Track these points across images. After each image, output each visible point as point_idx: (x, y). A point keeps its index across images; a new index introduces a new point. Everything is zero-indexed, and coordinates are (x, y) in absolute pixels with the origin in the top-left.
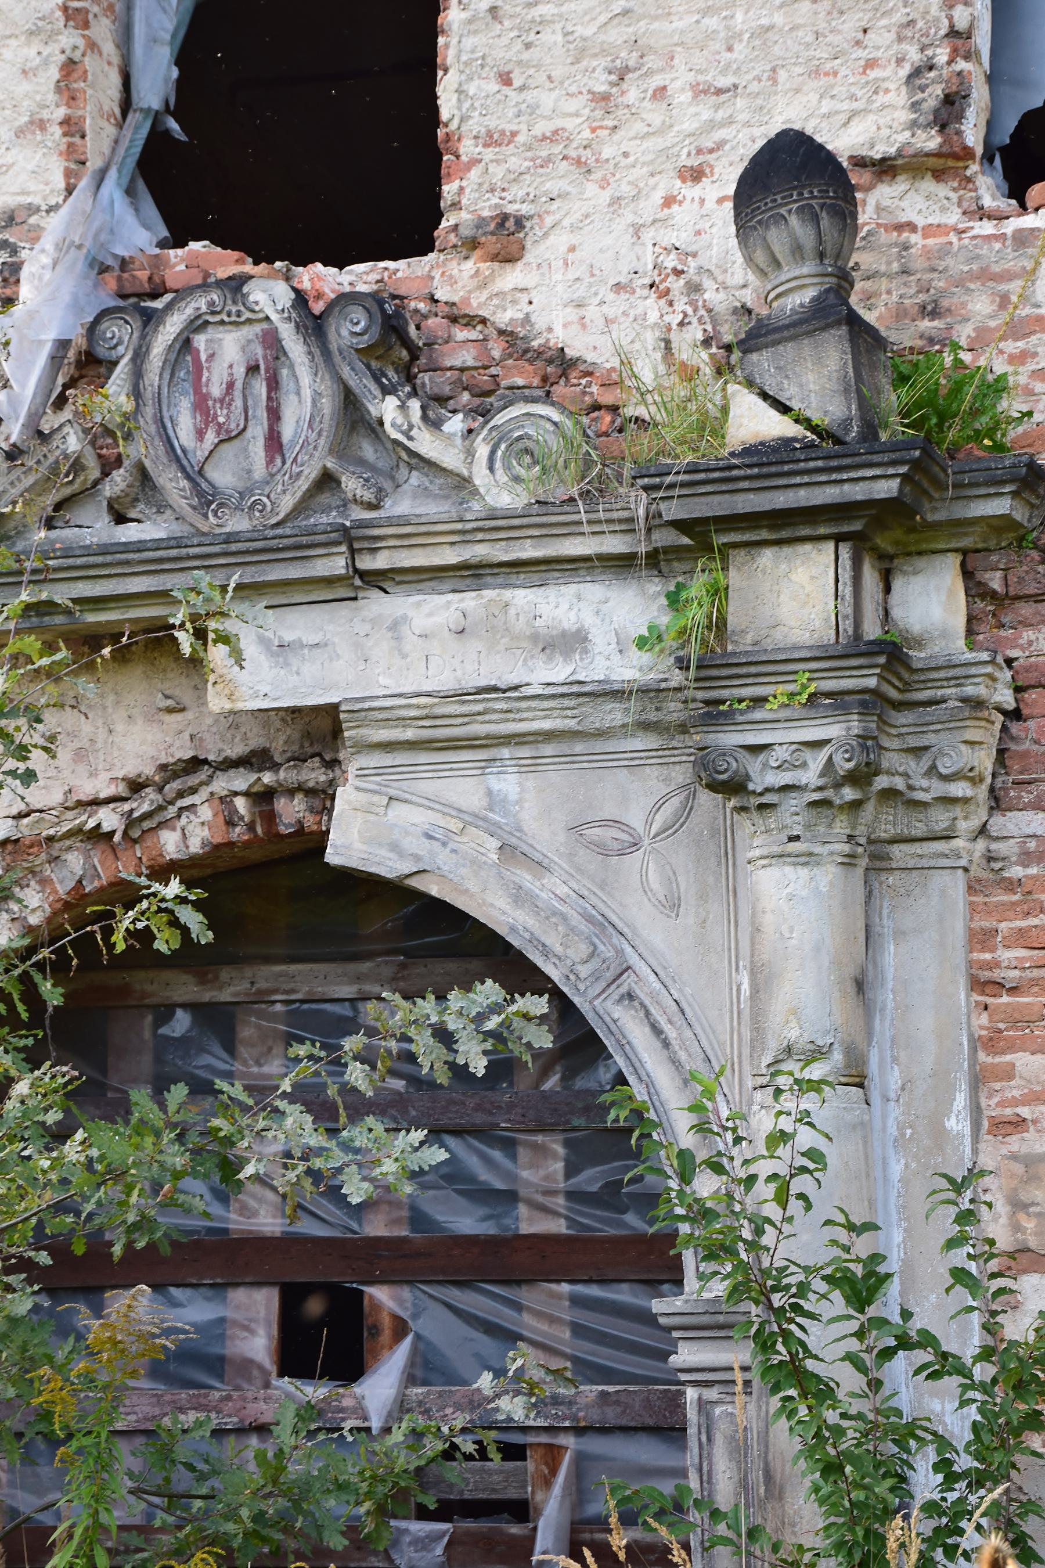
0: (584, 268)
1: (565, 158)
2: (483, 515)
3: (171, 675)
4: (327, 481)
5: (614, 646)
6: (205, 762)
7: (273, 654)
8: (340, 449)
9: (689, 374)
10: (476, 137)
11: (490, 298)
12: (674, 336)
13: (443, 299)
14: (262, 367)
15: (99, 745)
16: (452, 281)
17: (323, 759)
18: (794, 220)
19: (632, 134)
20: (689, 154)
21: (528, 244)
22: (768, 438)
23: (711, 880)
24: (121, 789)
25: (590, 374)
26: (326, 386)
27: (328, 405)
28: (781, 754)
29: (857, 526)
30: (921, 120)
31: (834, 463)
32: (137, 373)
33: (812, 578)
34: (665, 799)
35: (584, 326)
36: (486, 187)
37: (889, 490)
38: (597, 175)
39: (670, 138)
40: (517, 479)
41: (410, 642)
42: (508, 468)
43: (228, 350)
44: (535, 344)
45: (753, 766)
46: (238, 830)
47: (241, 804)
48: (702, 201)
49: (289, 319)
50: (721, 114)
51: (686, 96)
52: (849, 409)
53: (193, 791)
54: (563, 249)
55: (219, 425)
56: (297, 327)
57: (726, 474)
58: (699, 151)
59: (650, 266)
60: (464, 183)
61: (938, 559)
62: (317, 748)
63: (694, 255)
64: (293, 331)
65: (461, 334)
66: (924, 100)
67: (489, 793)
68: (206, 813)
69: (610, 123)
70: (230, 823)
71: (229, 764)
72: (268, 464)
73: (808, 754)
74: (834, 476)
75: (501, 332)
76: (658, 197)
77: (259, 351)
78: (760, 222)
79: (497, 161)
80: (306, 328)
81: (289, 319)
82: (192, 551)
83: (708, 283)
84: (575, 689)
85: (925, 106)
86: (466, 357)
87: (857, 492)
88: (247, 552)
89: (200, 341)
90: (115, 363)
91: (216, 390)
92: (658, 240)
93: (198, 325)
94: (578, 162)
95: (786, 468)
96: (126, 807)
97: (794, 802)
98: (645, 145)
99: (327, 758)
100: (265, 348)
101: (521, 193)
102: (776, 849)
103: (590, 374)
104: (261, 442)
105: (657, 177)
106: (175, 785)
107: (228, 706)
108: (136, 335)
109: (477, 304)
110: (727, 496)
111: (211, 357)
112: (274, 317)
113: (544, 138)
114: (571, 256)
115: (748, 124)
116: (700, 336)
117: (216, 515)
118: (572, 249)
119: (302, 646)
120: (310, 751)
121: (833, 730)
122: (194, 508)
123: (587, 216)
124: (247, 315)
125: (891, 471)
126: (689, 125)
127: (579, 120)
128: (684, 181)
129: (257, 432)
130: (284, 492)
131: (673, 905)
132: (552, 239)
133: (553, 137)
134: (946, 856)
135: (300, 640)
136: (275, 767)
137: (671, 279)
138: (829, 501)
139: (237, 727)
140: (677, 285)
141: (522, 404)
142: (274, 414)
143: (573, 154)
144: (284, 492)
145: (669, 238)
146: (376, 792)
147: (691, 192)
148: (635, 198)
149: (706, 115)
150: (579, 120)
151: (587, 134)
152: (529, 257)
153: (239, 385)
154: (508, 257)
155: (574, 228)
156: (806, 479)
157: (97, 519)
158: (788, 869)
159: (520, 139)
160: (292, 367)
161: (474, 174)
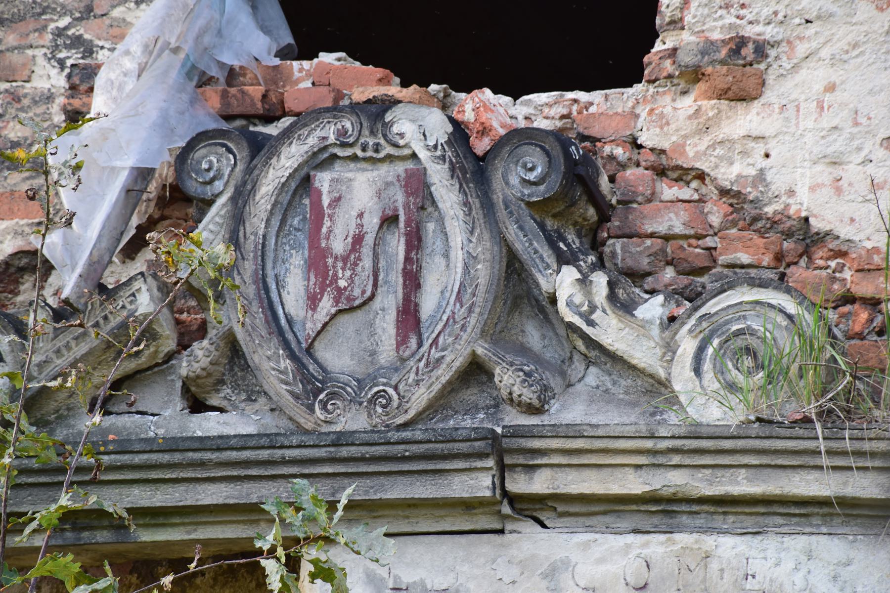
2: (682, 431)
11: (713, 146)
13: (649, 144)
14: (402, 218)
16: (663, 122)
21: (770, 78)
26: (485, 247)
27: (483, 272)
40: (732, 387)
42: (720, 371)
43: (359, 194)
44: (769, 210)
49: (443, 158)
54: (819, 87)
55: (340, 290)
56: (452, 169)
75: (724, 192)
77: (400, 198)
81: (443, 158)
86: (674, 222)
88: (362, 459)
89: (323, 180)
91: (339, 246)
100: (408, 194)
108: (240, 167)
109: (694, 153)
111: (336, 201)
112: (423, 154)
117: (324, 407)
118: (831, 88)
122: (296, 397)
124: (388, 150)
130: (417, 383)
132: (803, 74)
141: (745, 288)
152: (770, 95)
153: (369, 239)
154: (741, 95)
160: (441, 221)
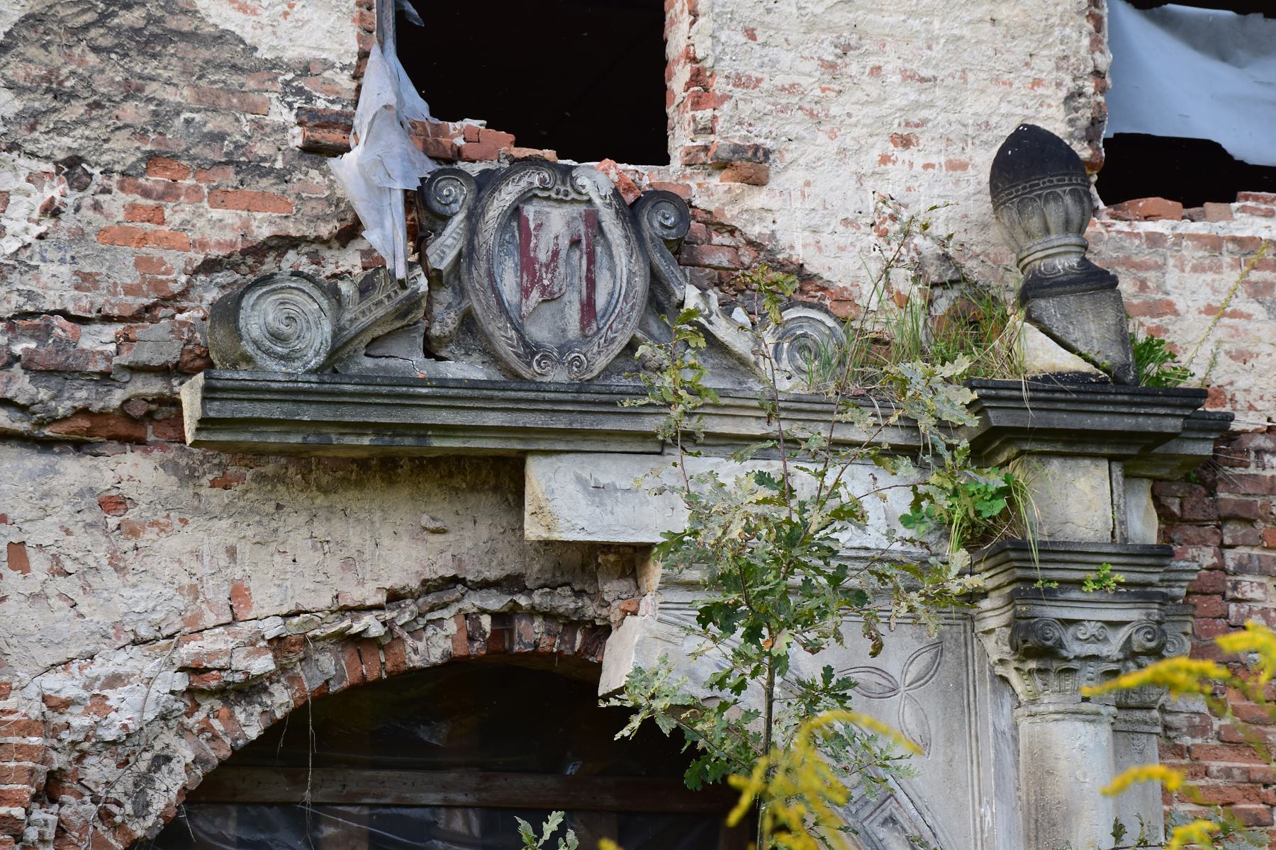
0: (818, 201)
1: (800, 108)
2: (791, 397)
3: (435, 499)
4: (632, 346)
5: (883, 521)
6: (463, 581)
9: (904, 301)
10: (727, 77)
11: (741, 213)
13: (702, 207)
14: (584, 242)
15: (366, 556)
16: (709, 193)
17: (573, 590)
18: (1068, 200)
19: (854, 99)
20: (899, 125)
21: (772, 173)
22: (1064, 371)
23: (956, 726)
24: (381, 598)
25: (823, 289)
26: (639, 268)
27: (640, 284)
28: (1092, 629)
29: (1133, 451)
30: (1076, 133)
31: (1138, 399)
32: (472, 228)
33: (1092, 487)
34: (917, 654)
35: (820, 249)
36: (735, 120)
37: (1175, 427)
38: (827, 127)
39: (884, 109)
40: (800, 370)
42: (791, 359)
43: (554, 224)
44: (780, 257)
45: (1068, 635)
46: (476, 644)
47: (486, 621)
48: (911, 164)
49: (610, 204)
50: (923, 98)
51: (897, 78)
52: (1127, 356)
53: (445, 606)
54: (800, 182)
55: (543, 286)
56: (617, 213)
57: (1050, 395)
58: (907, 124)
59: (872, 210)
60: (717, 113)
61: (1137, 482)
62: (567, 578)
63: (906, 207)
64: (614, 216)
65: (717, 239)
66: (1078, 119)
68: (451, 627)
69: (837, 88)
70: (471, 639)
71: (485, 585)
72: (583, 329)
73: (1109, 632)
74: (1133, 410)
75: (750, 243)
76: (875, 154)
77: (582, 229)
78: (1039, 196)
79: (744, 100)
80: (623, 213)
81: (610, 204)
82: (547, 395)
84: (862, 554)
85: (1078, 123)
86: (722, 259)
87: (1150, 425)
88: (594, 403)
89: (530, 211)
90: (445, 219)
91: (543, 257)
92: (877, 189)
94: (811, 114)
95: (1099, 397)
96: (388, 615)
97: (1093, 669)
98: (865, 111)
99: (576, 588)
100: (587, 227)
101: (765, 130)
102: (1071, 707)
103: (823, 289)
105: (875, 138)
106: (431, 599)
107: (545, 535)
108: (470, 196)
109: (730, 215)
110: (1044, 413)
111: (539, 226)
112: (598, 201)
113: (783, 89)
115: (945, 110)
117: (539, 364)
118: (808, 184)
120: (560, 580)
121: (1135, 615)
122: (519, 356)
123: (819, 159)
124: (573, 195)
125: (1179, 412)
126: (899, 102)
127: (812, 80)
128: (896, 146)
130: (599, 353)
132: (790, 173)
133: (791, 89)
134: (1146, 723)
135: (614, 484)
136: (524, 590)
137: (893, 222)
138: (1127, 428)
139: (494, 553)
141: (800, 308)
142: (591, 284)
143: (807, 106)
144: (599, 353)
145: (886, 190)
146: (676, 624)
147: (901, 154)
148: (857, 152)
149: (913, 96)
150: (812, 80)
151: (818, 92)
152: (772, 184)
153: (563, 254)
154: (757, 181)
155: (809, 167)
156: (1111, 409)
157: (411, 352)
158: (1079, 724)
159: (764, 85)
160: (608, 246)
161: (727, 107)
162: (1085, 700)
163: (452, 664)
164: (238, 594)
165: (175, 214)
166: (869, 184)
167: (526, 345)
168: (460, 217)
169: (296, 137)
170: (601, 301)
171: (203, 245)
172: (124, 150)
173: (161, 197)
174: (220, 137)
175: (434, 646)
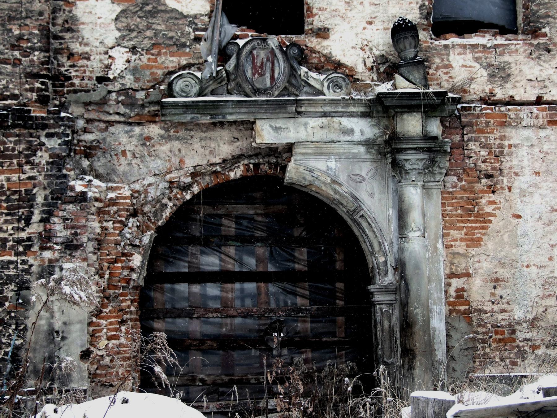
6: (244, 155)
7: (274, 130)
8: (289, 82)
12: (366, 60)
18: (410, 39)
28: (413, 161)
32: (238, 59)
41: (309, 129)
44: (333, 59)
47: (251, 166)
65: (314, 55)
67: (328, 166)
68: (242, 168)
70: (248, 171)
75: (324, 56)
77: (270, 56)
83: (374, 49)
86: (315, 61)
89: (255, 52)
93: (254, 48)
104: (269, 78)
109: (318, 48)
111: (257, 56)
112: (274, 48)
114: (341, 39)
116: (372, 61)
119: (281, 128)
129: (268, 75)
131: (372, 195)
140: (367, 48)
142: (273, 71)
145: (364, 37)
153: (264, 63)
154: (326, 37)
160: (278, 60)
162: (413, 181)
163: (243, 178)
164: (181, 161)
165: (161, 59)
166: (360, 36)
167: (254, 90)
168: (235, 55)
169: (192, 36)
170: (276, 75)
171: (168, 68)
172: (147, 43)
173: (157, 55)
174: (172, 38)
175: (236, 174)
